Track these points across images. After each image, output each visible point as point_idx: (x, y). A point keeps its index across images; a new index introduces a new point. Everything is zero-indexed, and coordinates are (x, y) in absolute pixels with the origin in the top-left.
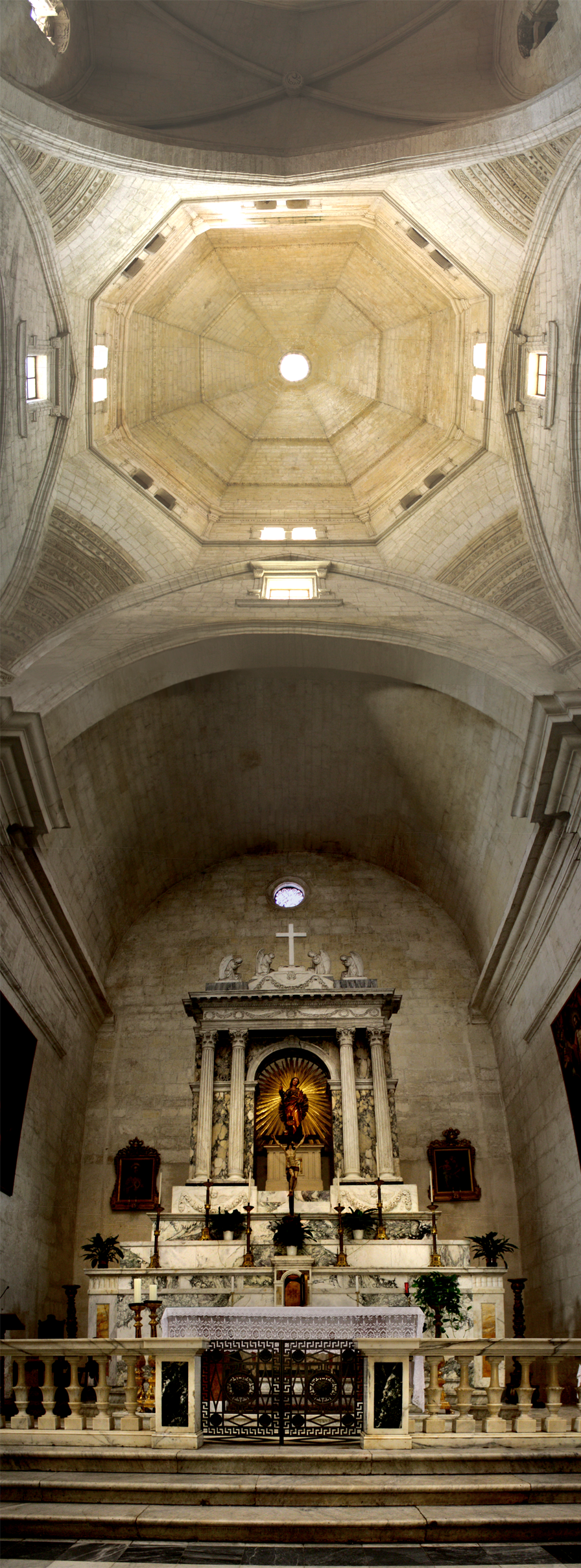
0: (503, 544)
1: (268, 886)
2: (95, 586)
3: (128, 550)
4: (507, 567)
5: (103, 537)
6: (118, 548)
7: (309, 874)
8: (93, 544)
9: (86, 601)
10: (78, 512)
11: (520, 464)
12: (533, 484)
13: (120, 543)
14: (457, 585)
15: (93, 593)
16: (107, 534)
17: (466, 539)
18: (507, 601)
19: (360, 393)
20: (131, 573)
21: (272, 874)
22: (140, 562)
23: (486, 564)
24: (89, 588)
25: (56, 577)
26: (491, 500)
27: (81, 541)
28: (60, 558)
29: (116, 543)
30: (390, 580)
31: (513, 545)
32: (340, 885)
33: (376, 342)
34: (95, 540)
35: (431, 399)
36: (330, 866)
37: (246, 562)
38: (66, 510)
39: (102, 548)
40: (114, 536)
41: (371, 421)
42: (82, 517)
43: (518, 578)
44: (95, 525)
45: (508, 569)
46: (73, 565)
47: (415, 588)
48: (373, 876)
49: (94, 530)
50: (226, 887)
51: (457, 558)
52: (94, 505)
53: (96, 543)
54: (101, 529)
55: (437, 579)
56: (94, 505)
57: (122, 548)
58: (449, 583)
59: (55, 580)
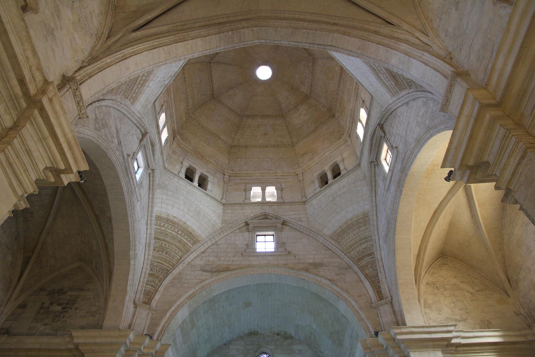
0: (361, 227)
1: (255, 353)
2: (177, 252)
3: (190, 226)
4: (361, 240)
5: (179, 222)
6: (186, 226)
7: (273, 347)
8: (175, 227)
9: (174, 260)
10: (167, 213)
11: (372, 191)
12: (377, 203)
13: (187, 223)
14: (339, 242)
15: (177, 256)
16: (180, 220)
17: (345, 219)
18: (359, 260)
19: (300, 90)
20: (194, 238)
21: (256, 346)
22: (197, 231)
23: (353, 235)
24: (175, 254)
25: (160, 252)
26: (358, 202)
27: (169, 227)
28: (160, 244)
29: (185, 223)
30: (311, 234)
31: (365, 229)
32: (287, 354)
33: (310, 65)
34: (176, 225)
35: (338, 106)
36: (283, 342)
37: (245, 221)
38: (161, 214)
39: (179, 228)
40: (184, 220)
41: (306, 107)
42: (168, 215)
43: (365, 249)
44: (175, 217)
45: (361, 242)
46: (166, 245)
47: (321, 241)
48: (302, 348)
49: (175, 220)
50: (236, 353)
51: (340, 227)
52: (173, 206)
53: (176, 226)
54: (177, 218)
55: (331, 237)
56: (173, 206)
57: (188, 225)
58: (336, 241)
59: (160, 254)
